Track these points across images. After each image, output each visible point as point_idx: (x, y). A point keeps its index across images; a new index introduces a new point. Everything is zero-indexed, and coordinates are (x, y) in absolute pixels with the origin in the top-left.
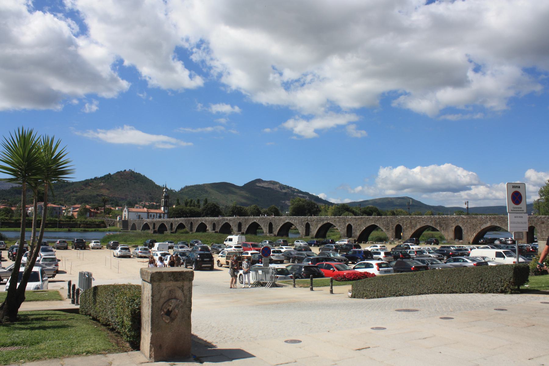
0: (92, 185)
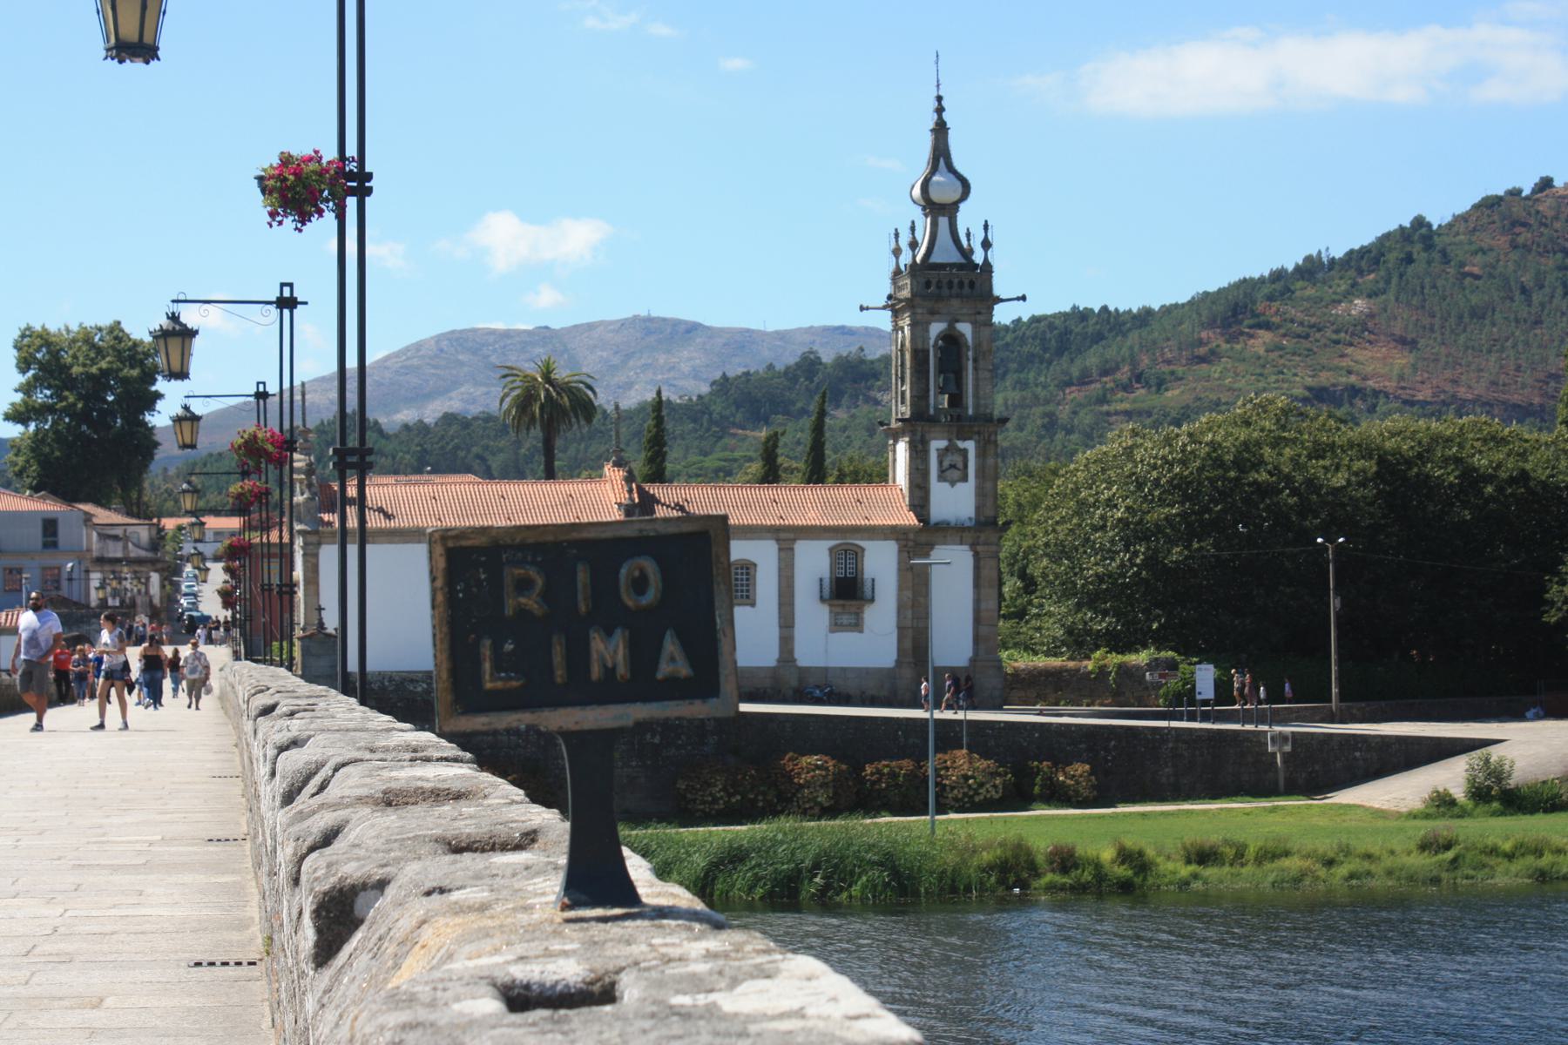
0: (1276, 320)
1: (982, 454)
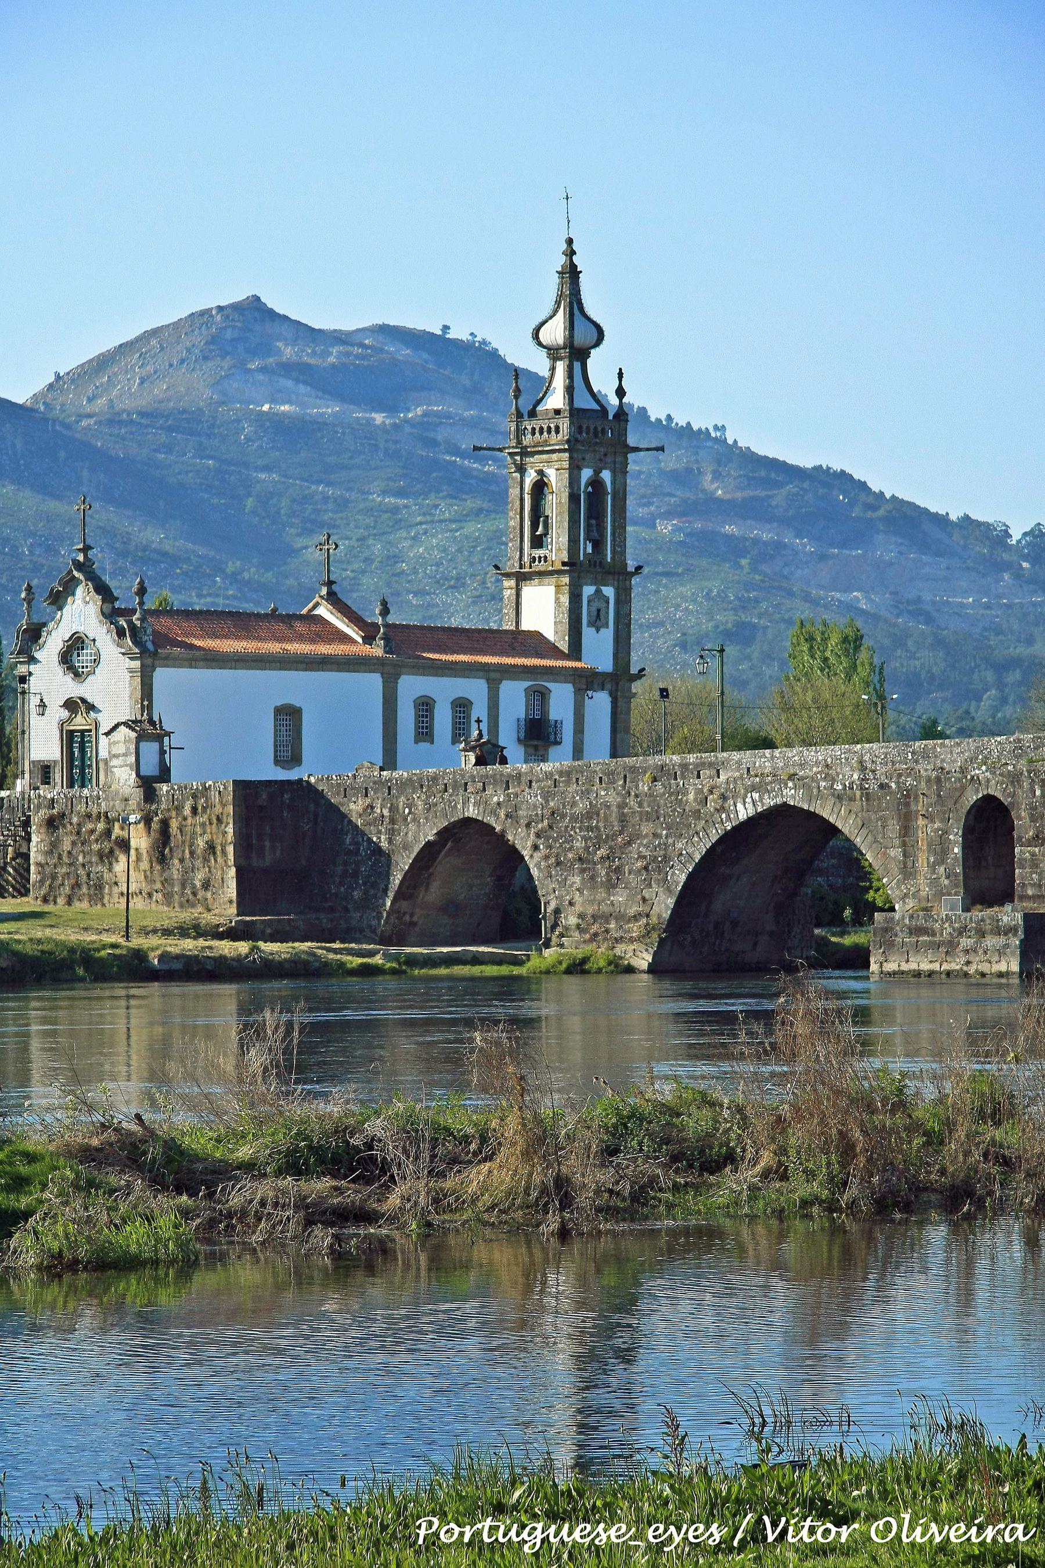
1: (617, 602)
